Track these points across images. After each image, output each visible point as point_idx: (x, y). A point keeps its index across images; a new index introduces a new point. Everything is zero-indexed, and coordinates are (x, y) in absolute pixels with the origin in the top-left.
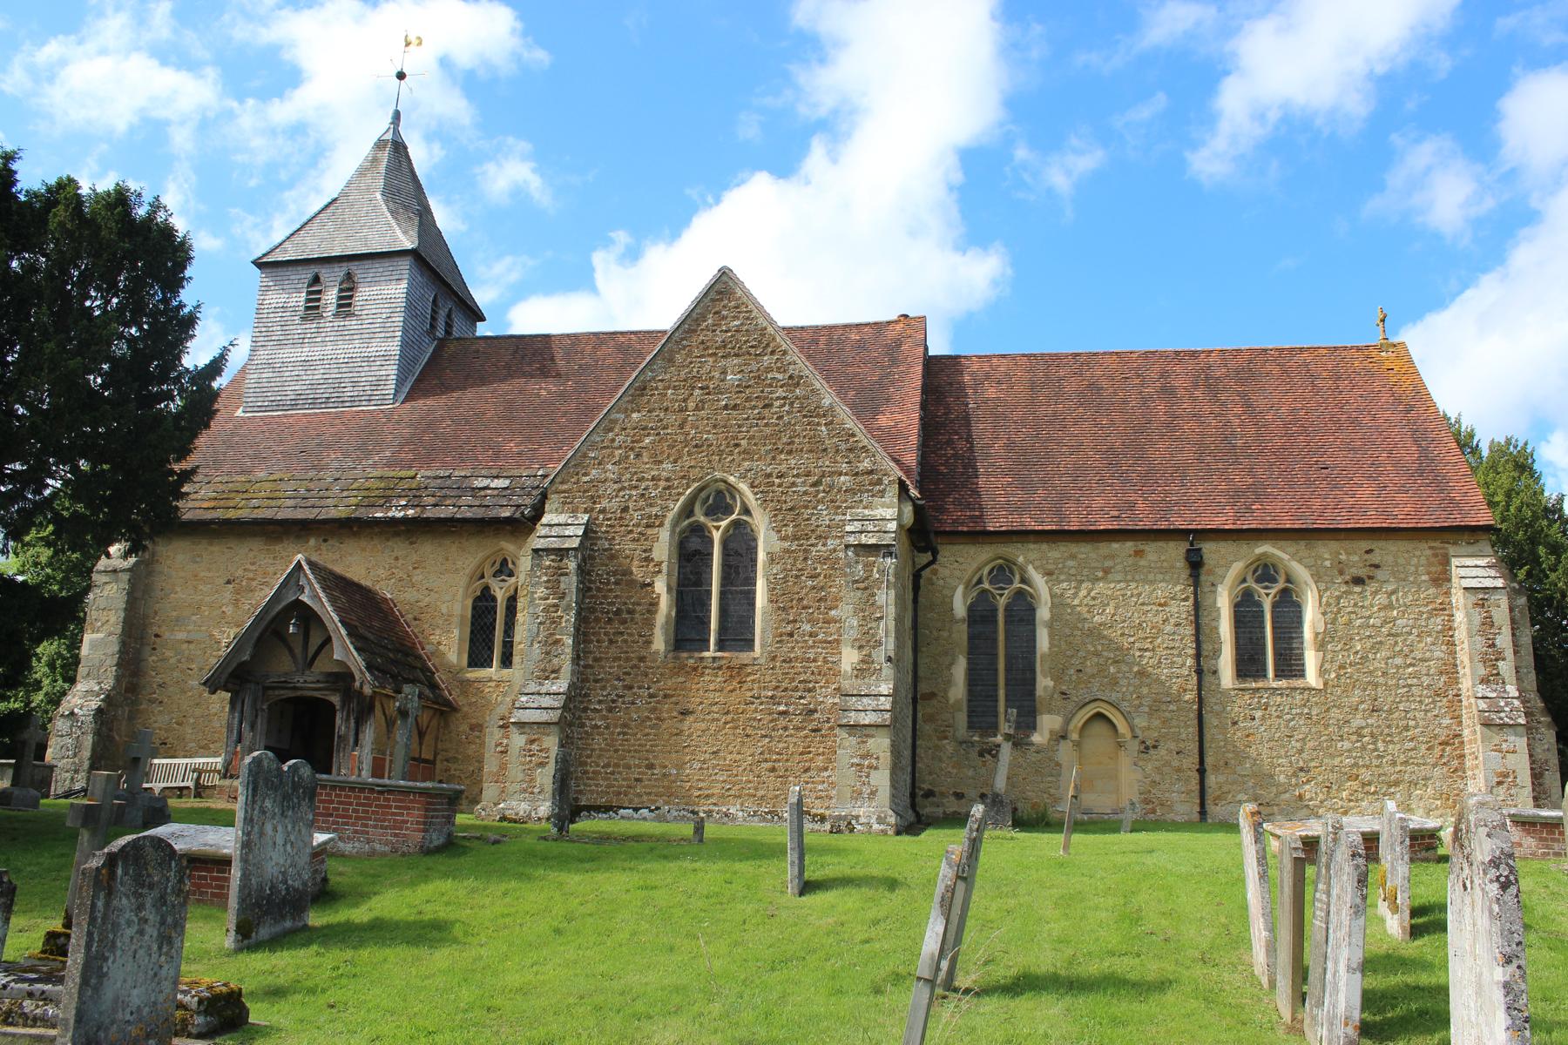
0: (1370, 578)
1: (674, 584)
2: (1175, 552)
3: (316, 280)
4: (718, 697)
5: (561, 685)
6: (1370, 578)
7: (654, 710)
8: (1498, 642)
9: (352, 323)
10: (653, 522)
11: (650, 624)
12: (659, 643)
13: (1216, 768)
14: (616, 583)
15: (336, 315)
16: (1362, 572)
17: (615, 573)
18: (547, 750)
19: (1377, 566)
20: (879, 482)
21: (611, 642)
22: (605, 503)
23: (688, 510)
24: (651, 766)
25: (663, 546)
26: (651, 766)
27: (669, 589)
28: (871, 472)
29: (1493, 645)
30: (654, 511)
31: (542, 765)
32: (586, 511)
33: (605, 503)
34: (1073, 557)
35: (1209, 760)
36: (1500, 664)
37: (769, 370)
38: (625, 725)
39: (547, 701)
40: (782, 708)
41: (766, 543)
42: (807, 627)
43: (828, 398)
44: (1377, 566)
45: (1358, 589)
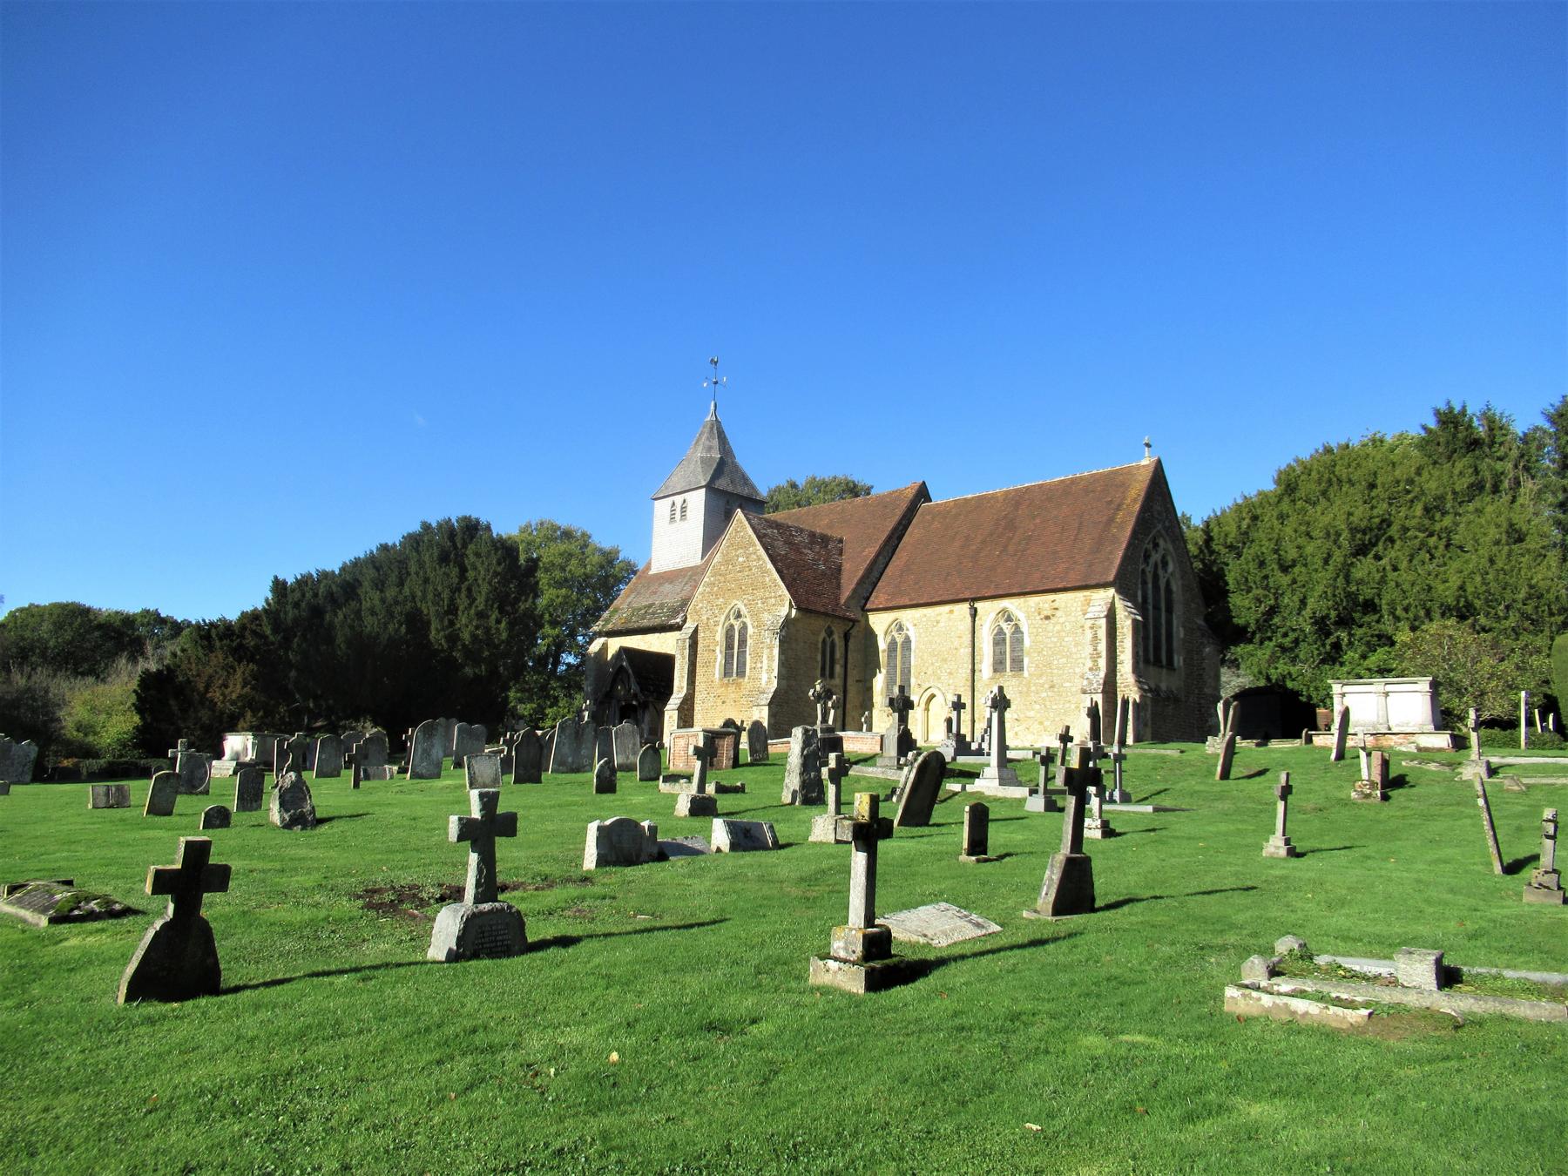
2: (965, 607)
16: (1049, 613)
23: (728, 617)
25: (720, 635)
41: (750, 631)
43: (770, 566)
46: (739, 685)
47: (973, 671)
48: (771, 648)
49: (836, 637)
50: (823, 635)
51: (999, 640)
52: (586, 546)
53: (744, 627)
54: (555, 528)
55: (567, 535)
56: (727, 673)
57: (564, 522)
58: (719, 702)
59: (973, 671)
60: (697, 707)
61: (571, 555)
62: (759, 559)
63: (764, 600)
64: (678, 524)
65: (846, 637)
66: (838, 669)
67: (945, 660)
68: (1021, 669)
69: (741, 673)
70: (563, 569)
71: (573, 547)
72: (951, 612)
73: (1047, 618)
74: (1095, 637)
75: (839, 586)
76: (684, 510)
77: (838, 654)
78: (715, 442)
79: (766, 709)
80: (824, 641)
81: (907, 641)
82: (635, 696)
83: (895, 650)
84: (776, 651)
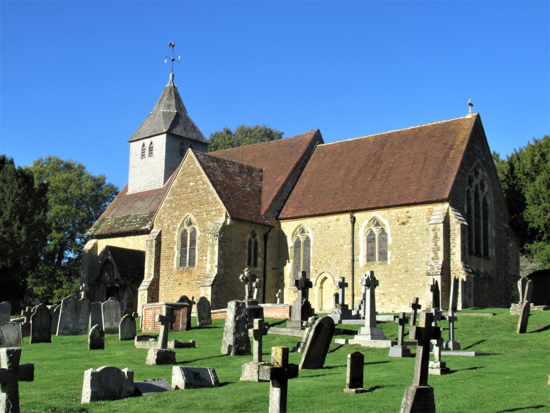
0: (407, 222)
3: (144, 145)
4: (186, 279)
5: (151, 279)
6: (407, 222)
7: (174, 284)
8: (438, 244)
9: (151, 160)
10: (174, 229)
11: (173, 260)
12: (175, 266)
13: (358, 294)
15: (149, 156)
19: (410, 217)
23: (182, 225)
25: (177, 237)
27: (178, 249)
28: (219, 210)
29: (436, 245)
34: (320, 223)
35: (355, 292)
36: (439, 252)
40: (199, 282)
41: (198, 234)
43: (212, 188)
44: (410, 217)
45: (403, 226)
46: (190, 272)
47: (353, 261)
48: (213, 246)
49: (258, 238)
50: (249, 236)
51: (370, 239)
52: (81, 174)
53: (194, 232)
54: (59, 162)
55: (68, 167)
56: (182, 263)
57: (65, 158)
58: (177, 284)
59: (353, 261)
60: (161, 288)
61: (71, 181)
62: (204, 183)
63: (208, 212)
64: (147, 159)
65: (265, 238)
66: (260, 260)
67: (333, 254)
68: (386, 259)
70: (65, 191)
71: (72, 175)
72: (338, 220)
73: (403, 223)
74: (436, 237)
75: (260, 203)
76: (151, 149)
77: (260, 250)
78: (173, 102)
79: (210, 289)
80: (250, 241)
81: (308, 240)
82: (117, 280)
83: (299, 247)
84: (216, 248)
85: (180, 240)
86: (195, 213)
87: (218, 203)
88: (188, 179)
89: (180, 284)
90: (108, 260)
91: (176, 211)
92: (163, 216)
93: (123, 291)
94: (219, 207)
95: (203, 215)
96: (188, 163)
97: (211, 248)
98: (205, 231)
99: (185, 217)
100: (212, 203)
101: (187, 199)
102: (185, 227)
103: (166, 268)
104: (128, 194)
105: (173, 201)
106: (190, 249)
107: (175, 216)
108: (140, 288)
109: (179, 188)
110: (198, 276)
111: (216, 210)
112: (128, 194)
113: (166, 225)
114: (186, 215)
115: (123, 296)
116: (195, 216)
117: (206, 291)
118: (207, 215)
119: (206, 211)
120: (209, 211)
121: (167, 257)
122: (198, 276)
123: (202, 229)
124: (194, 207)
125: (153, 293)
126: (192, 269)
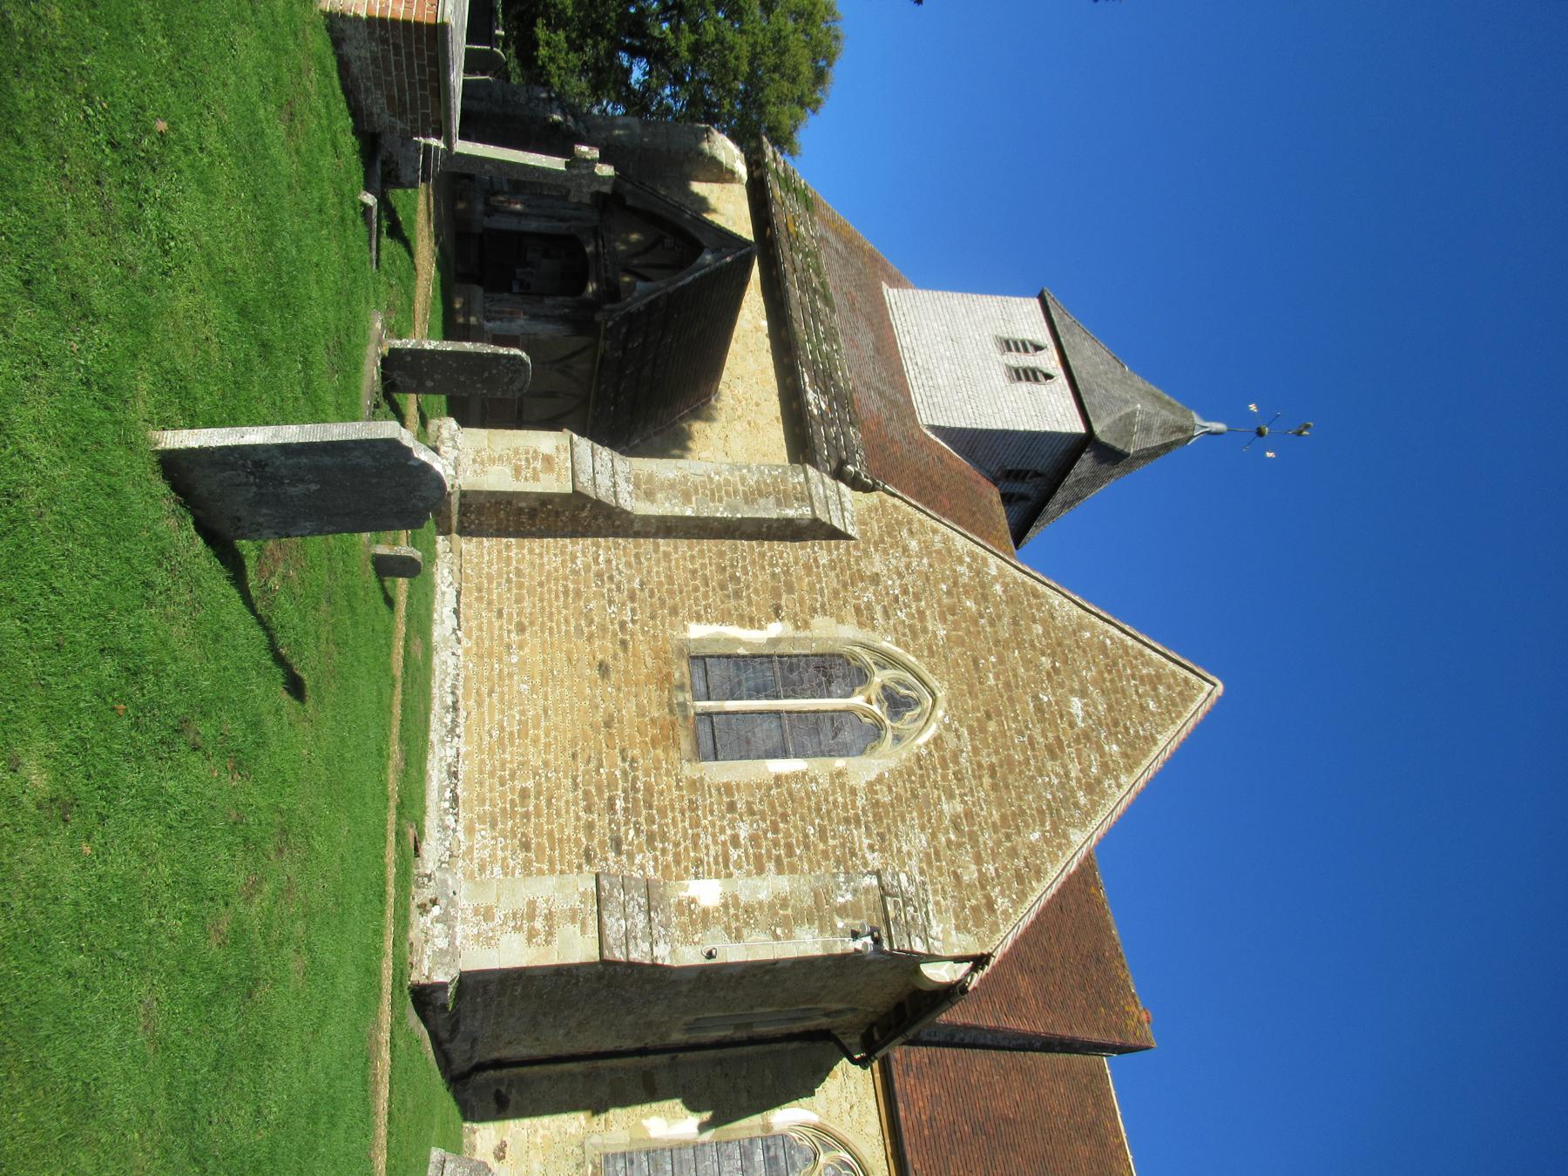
1: (785, 649)
3: (1038, 348)
4: (629, 710)
7: (603, 628)
9: (1000, 379)
10: (864, 616)
11: (725, 618)
12: (698, 631)
14: (773, 575)
15: (1009, 368)
17: (787, 573)
18: (536, 478)
20: (979, 923)
21: (694, 572)
22: (877, 557)
23: (887, 660)
24: (521, 629)
25: (832, 632)
26: (521, 629)
27: (774, 642)
28: (990, 905)
30: (879, 615)
31: (517, 471)
32: (863, 534)
33: (877, 557)
37: (1100, 749)
38: (578, 594)
39: (604, 481)
40: (619, 804)
41: (862, 770)
42: (744, 832)
46: (666, 738)
48: (818, 913)
52: (801, 103)
54: (830, 58)
55: (820, 77)
57: (837, 74)
58: (605, 648)
61: (794, 81)
69: (718, 739)
70: (776, 68)
71: (804, 86)
76: (1031, 375)
78: (1156, 441)
82: (612, 293)
84: (808, 943)
85: (815, 648)
86: (951, 741)
87: (1022, 896)
88: (1095, 683)
89: (603, 669)
90: (698, 249)
91: (944, 620)
92: (913, 545)
93: (563, 319)
94: (1001, 903)
95: (951, 796)
96: (1159, 677)
97: (809, 901)
98: (878, 818)
99: (927, 676)
100: (1013, 853)
101: (1007, 685)
102: (880, 677)
103: (680, 576)
104: (885, 286)
105: (985, 597)
106: (777, 713)
107: (921, 614)
108: (584, 445)
109: (1046, 634)
110: (649, 789)
111: (983, 881)
112: (885, 286)
113: (877, 565)
114: (934, 682)
115: (547, 318)
116: (937, 741)
117: (573, 916)
118: (957, 827)
119: (969, 815)
120: (973, 838)
121: (734, 578)
122: (649, 789)
123: (885, 798)
124: (977, 731)
125: (557, 514)
126: (686, 744)
